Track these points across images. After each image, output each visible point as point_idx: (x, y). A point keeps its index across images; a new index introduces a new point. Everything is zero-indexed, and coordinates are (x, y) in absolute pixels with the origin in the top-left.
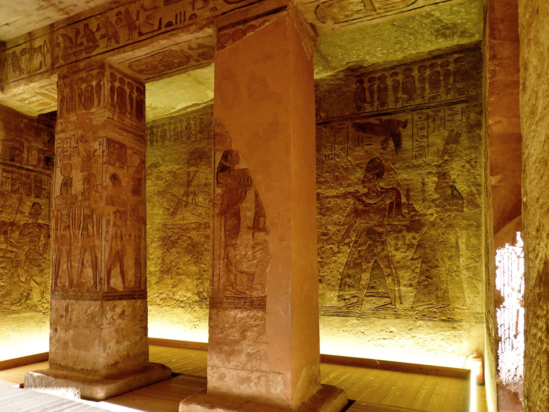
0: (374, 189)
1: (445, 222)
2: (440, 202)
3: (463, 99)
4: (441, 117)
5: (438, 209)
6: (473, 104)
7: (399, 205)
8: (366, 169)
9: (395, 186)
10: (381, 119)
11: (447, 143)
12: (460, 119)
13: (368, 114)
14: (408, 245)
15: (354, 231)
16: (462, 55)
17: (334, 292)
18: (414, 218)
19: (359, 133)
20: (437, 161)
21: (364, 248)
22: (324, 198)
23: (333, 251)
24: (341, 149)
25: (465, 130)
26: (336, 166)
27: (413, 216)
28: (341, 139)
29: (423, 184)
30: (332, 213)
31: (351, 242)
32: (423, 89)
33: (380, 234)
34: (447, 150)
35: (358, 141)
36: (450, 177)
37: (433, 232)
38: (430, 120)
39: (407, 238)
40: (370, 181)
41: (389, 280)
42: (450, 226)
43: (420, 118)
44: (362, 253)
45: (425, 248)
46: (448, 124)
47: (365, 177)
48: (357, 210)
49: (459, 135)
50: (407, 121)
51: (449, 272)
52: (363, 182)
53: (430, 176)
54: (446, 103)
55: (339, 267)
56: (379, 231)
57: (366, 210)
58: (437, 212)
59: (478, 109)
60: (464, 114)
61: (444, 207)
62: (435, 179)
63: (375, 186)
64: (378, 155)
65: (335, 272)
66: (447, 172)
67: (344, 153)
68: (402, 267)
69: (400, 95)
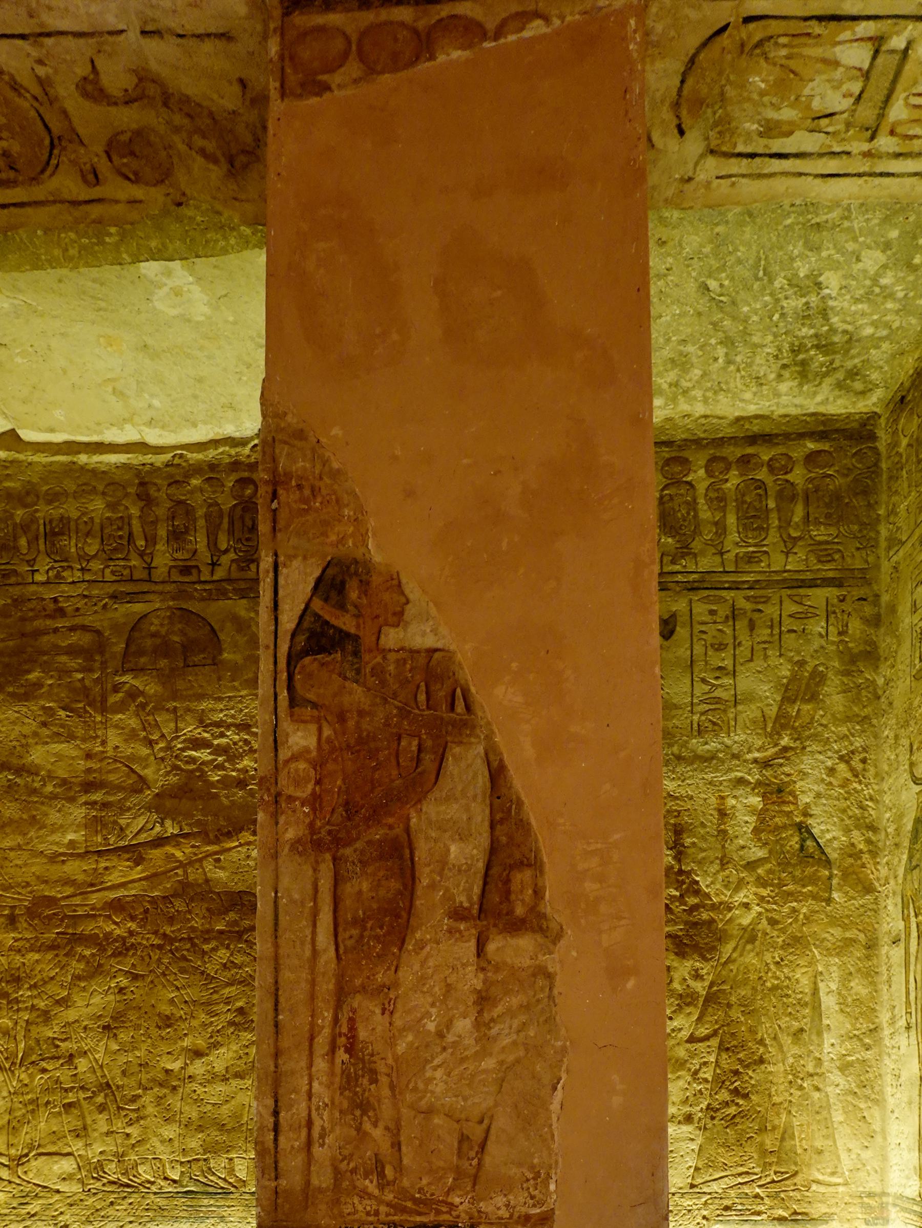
1: (783, 931)
2: (770, 871)
3: (831, 574)
4: (772, 620)
5: (764, 892)
6: (857, 593)
11: (788, 699)
12: (824, 633)
14: (681, 995)
16: (825, 446)
18: (695, 917)
20: (758, 747)
25: (836, 664)
32: (721, 528)
36: (795, 797)
37: (750, 959)
38: (742, 624)
39: (677, 976)
42: (796, 942)
43: (712, 612)
45: (729, 1006)
46: (790, 640)
49: (818, 678)
50: (674, 616)
53: (739, 792)
54: (785, 580)
58: (762, 898)
59: (868, 610)
60: (832, 619)
61: (781, 885)
62: (756, 801)
66: (788, 783)
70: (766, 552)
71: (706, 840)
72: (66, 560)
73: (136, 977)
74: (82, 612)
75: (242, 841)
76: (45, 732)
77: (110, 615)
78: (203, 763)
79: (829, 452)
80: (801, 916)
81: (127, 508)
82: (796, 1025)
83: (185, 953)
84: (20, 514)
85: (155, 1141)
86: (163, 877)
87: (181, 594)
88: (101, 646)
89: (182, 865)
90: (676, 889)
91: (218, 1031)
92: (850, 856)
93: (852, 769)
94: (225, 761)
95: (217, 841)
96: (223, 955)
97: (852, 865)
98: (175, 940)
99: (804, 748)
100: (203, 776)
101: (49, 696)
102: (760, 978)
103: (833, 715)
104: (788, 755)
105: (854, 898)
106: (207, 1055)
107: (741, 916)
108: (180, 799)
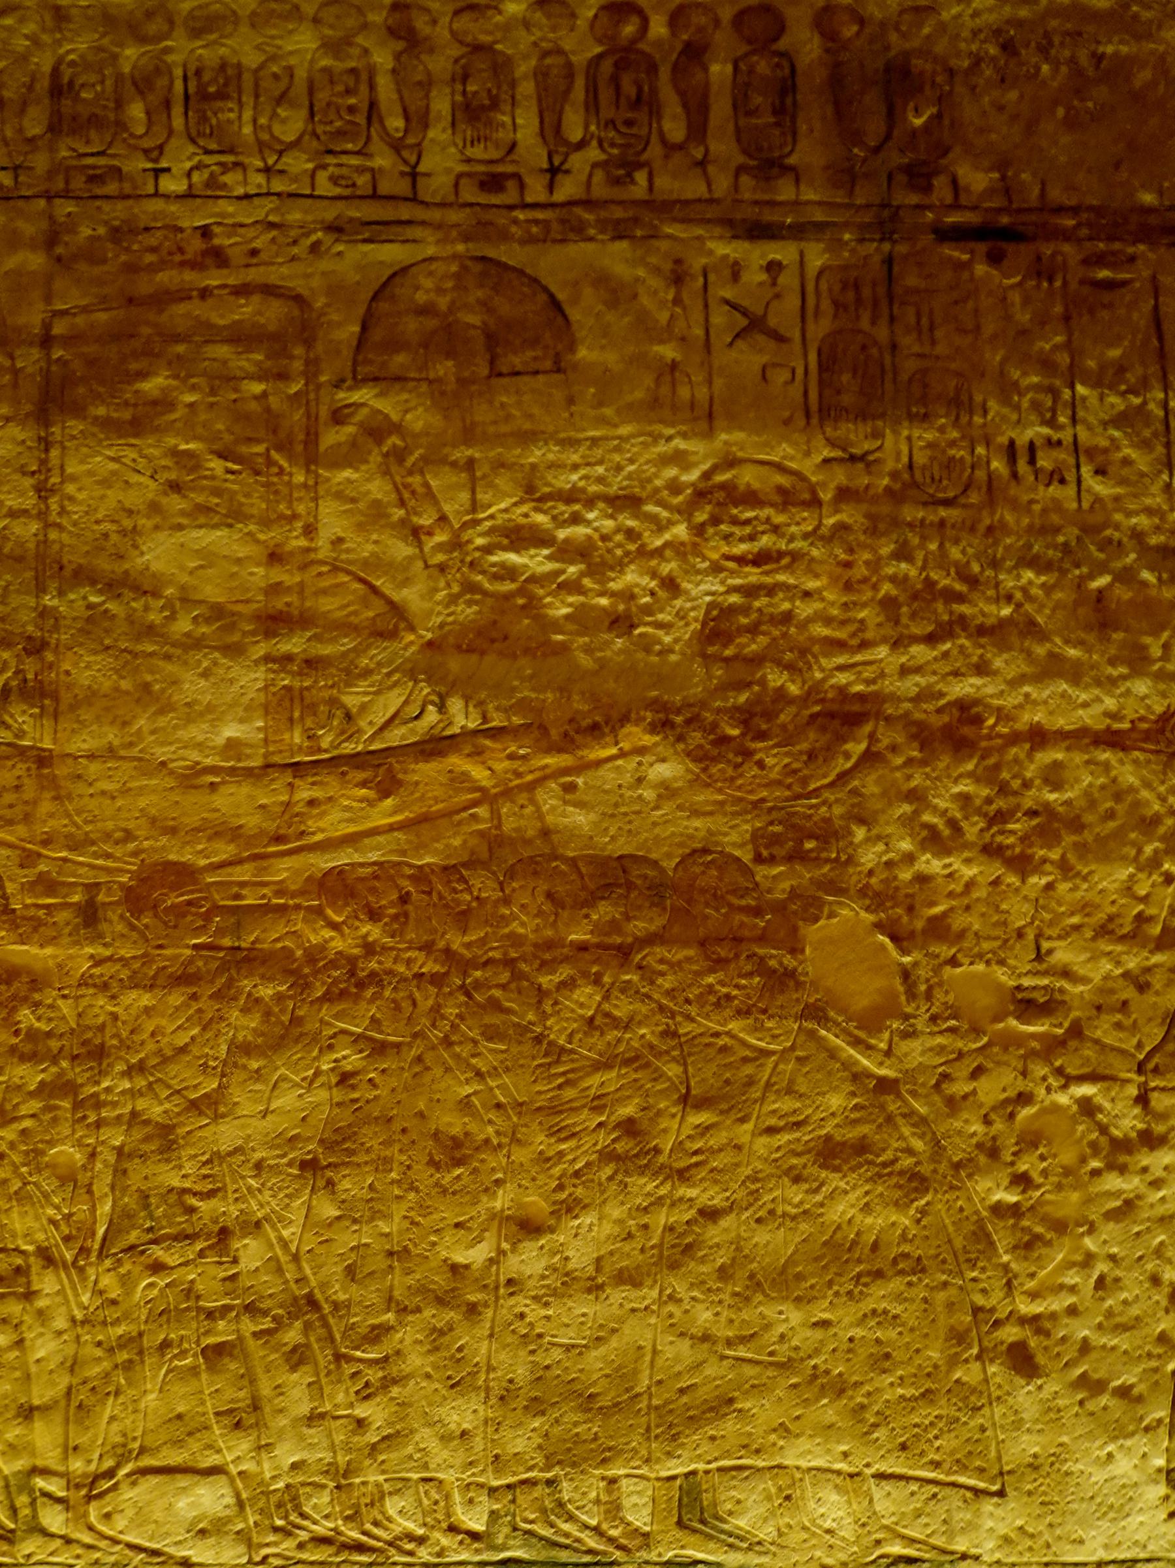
22: (1015, 738)
23: (1103, 1130)
24: (1121, 420)
28: (1115, 353)
65: (1133, 1287)
67: (1145, 445)
72: (231, 151)
73: (380, 1049)
74: (263, 256)
75: (625, 745)
76: (176, 503)
77: (324, 265)
78: (533, 579)
81: (366, 51)
83: (497, 993)
84: (131, 53)
85: (426, 1437)
86: (444, 822)
87: (482, 230)
88: (307, 327)
89: (484, 796)
91: (577, 1174)
94: (582, 574)
95: (566, 744)
96: (586, 998)
98: (472, 964)
100: (532, 607)
101: (189, 430)
106: (552, 1230)
108: (483, 653)
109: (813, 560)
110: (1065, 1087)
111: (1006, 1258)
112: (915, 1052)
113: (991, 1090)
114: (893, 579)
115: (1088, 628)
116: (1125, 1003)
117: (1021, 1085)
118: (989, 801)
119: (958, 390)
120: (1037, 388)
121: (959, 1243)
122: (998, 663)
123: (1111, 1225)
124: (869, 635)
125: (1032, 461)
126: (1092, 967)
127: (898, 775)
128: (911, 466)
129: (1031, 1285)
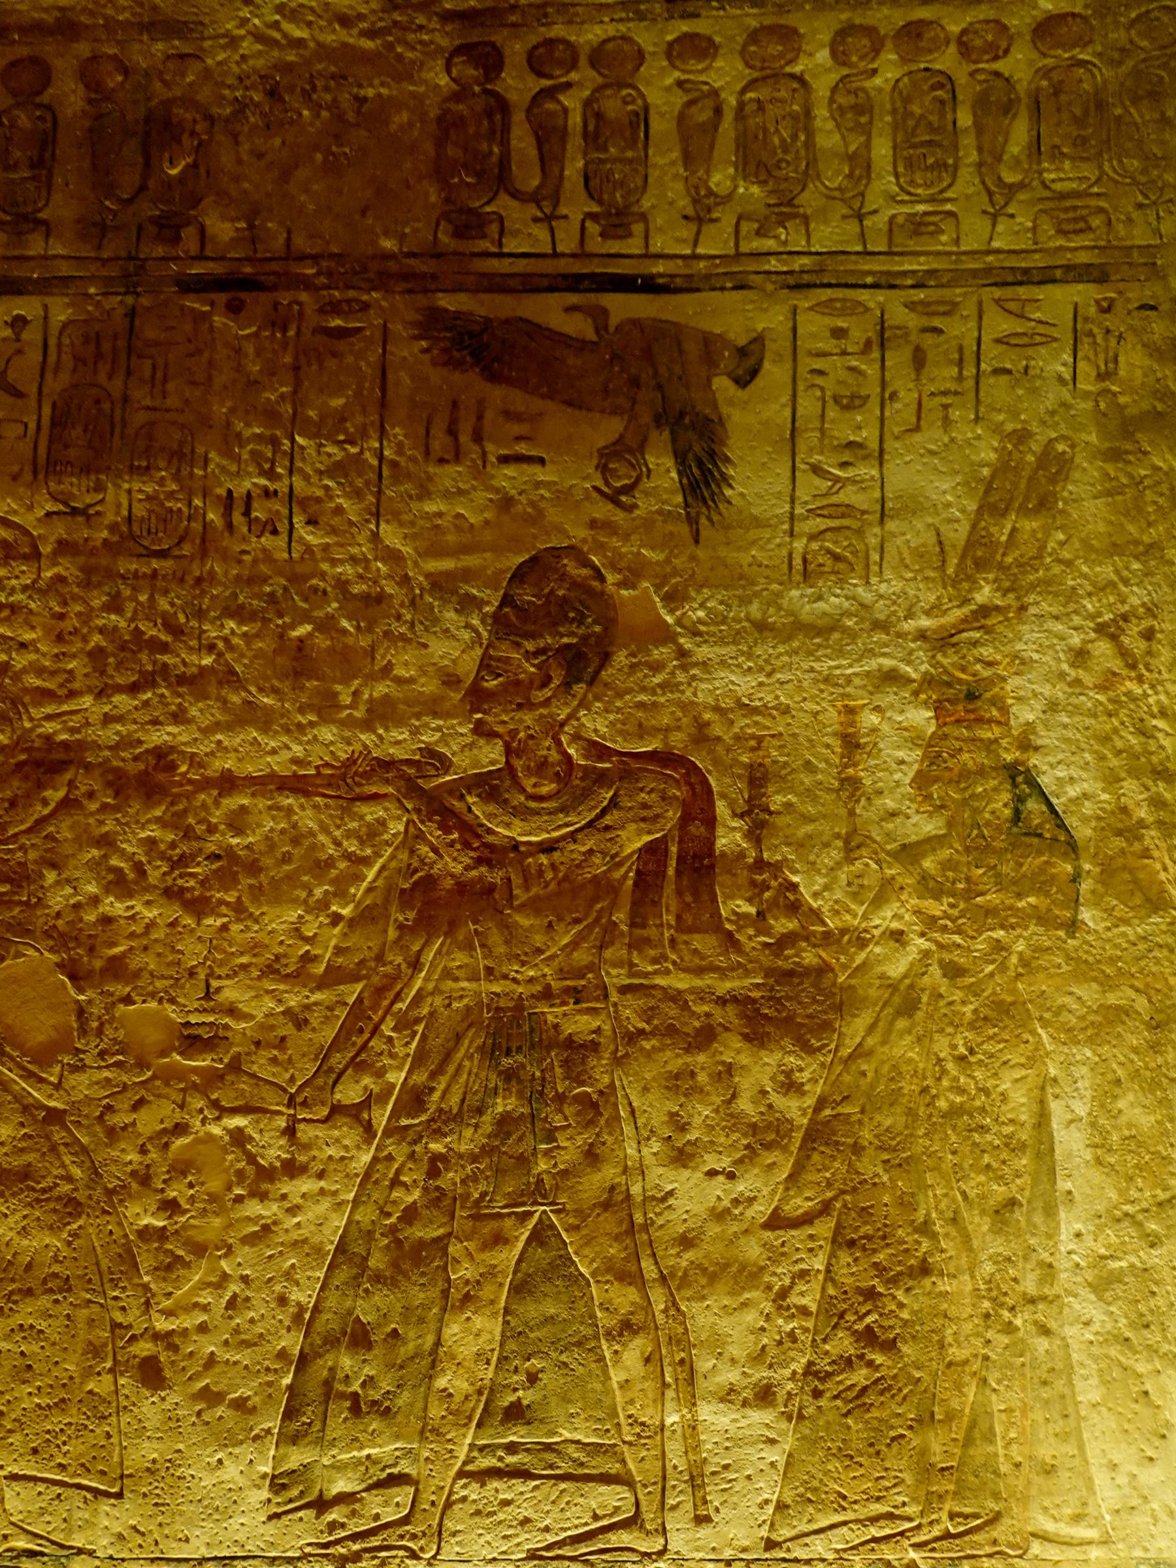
0: (545, 748)
1: (974, 990)
3: (1083, 258)
4: (961, 349)
6: (1135, 294)
7: (701, 865)
8: (497, 617)
9: (678, 741)
10: (605, 312)
12: (1068, 376)
13: (521, 266)
14: (754, 1126)
15: (405, 1024)
17: (246, 1451)
18: (790, 959)
19: (457, 377)
21: (466, 1141)
24: (337, 469)
25: (1093, 438)
26: (296, 579)
27: (786, 941)
28: (337, 402)
29: (851, 744)
30: (257, 892)
31: (383, 1097)
33: (578, 1052)
34: (990, 544)
35: (452, 432)
36: (1004, 710)
37: (904, 1049)
38: (899, 358)
39: (746, 1084)
40: (519, 693)
41: (628, 1361)
42: (1002, 1014)
44: (450, 1178)
45: (857, 1149)
46: (996, 390)
47: (486, 665)
48: (429, 882)
49: (1055, 466)
51: (998, 1304)
52: (477, 697)
53: (888, 698)
54: (988, 270)
55: (288, 1275)
56: (568, 1029)
57: (491, 889)
58: (931, 922)
60: (1085, 349)
61: (970, 893)
62: (921, 717)
63: (554, 729)
64: (579, 533)
65: (260, 1306)
66: (990, 682)
67: (358, 494)
68: (713, 1274)
69: (720, 179)
70: (950, 214)
71: (815, 799)
79: (1084, 19)
80: (1014, 959)
82: (1000, 1191)
90: (750, 900)
92: (1119, 833)
93: (1123, 653)
97: (1123, 852)
99: (1023, 608)
102: (925, 1090)
103: (1085, 543)
104: (989, 622)
105: (1126, 922)
107: (887, 958)
109: (31, 611)
110: (218, 1118)
111: (146, 1279)
112: (82, 1085)
113: (149, 1121)
114: (101, 631)
115: (284, 676)
116: (283, 1039)
117: (178, 1116)
118: (173, 845)
119: (182, 443)
120: (259, 438)
121: (105, 1263)
122: (194, 712)
123: (247, 1249)
124: (76, 685)
125: (247, 513)
126: (255, 1004)
127: (91, 820)
128: (129, 519)
129: (167, 1303)
